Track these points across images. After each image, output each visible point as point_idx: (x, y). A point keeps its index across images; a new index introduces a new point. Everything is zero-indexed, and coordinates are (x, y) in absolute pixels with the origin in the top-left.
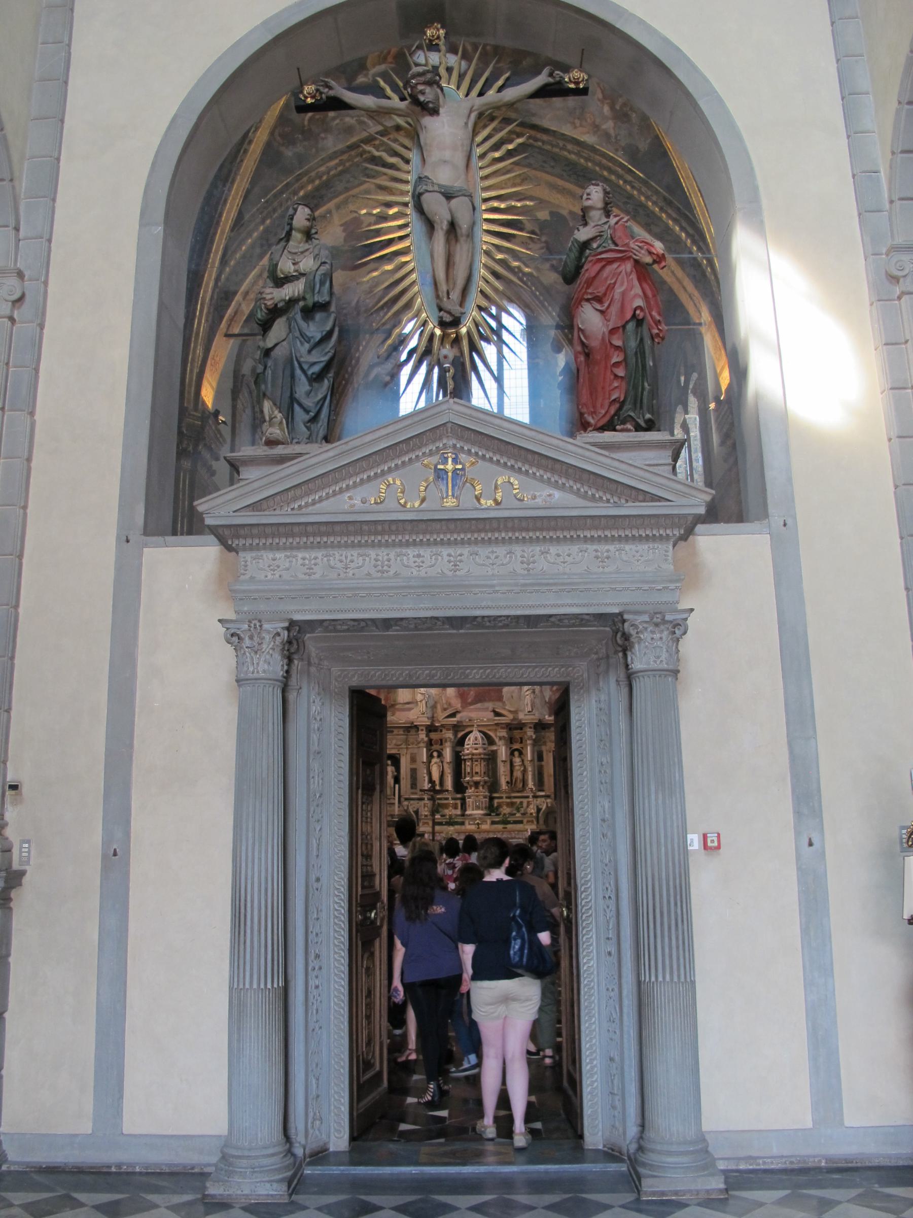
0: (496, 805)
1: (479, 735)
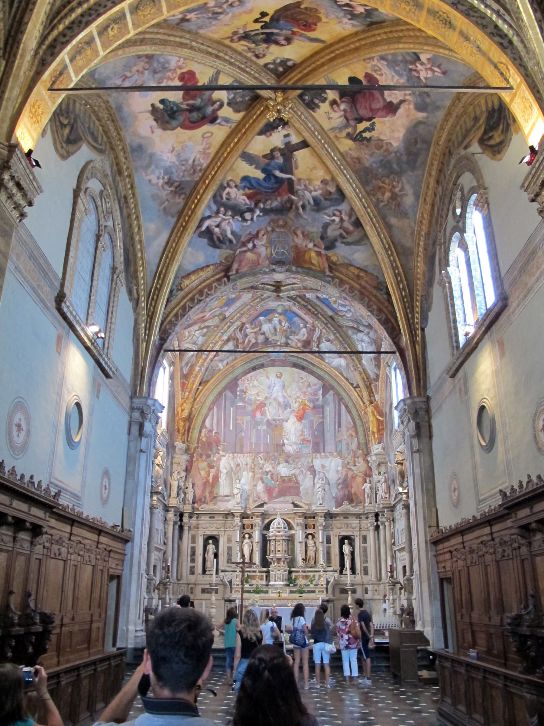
0: (293, 578)
1: (282, 521)
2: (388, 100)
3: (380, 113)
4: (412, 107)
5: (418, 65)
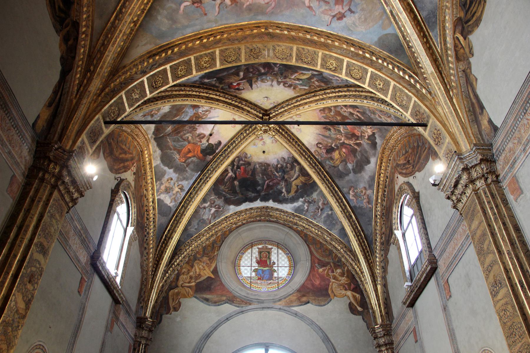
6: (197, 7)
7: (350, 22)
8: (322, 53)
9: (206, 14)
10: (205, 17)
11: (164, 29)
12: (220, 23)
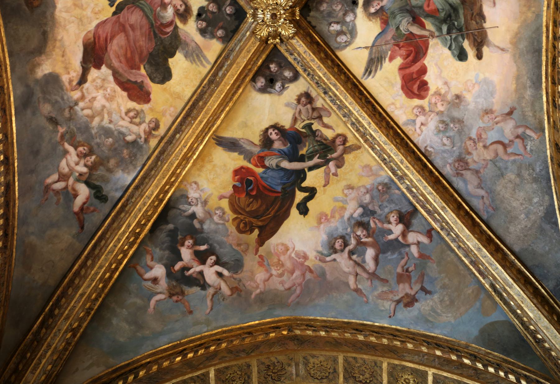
2: (104, 67)
3: (108, 28)
4: (65, 78)
5: (85, 170)
6: (177, 301)
7: (427, 308)
8: (389, 364)
9: (191, 312)
10: (190, 317)
11: (122, 340)
12: (214, 325)
